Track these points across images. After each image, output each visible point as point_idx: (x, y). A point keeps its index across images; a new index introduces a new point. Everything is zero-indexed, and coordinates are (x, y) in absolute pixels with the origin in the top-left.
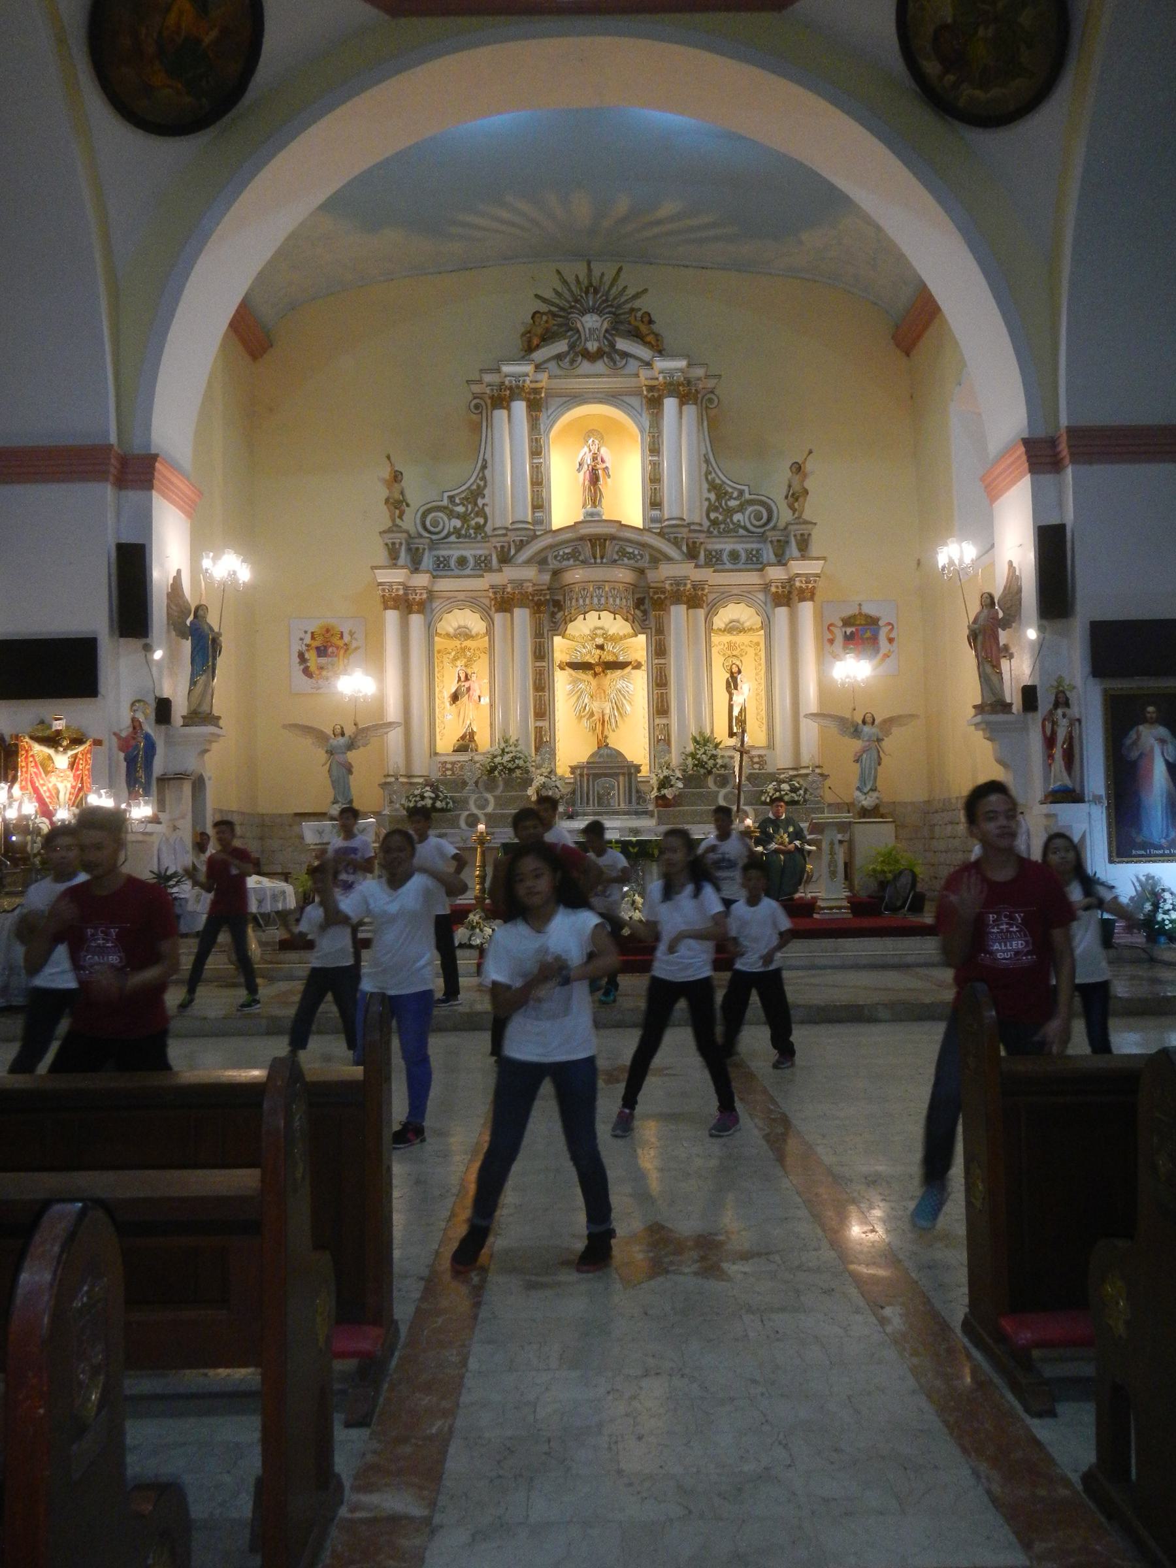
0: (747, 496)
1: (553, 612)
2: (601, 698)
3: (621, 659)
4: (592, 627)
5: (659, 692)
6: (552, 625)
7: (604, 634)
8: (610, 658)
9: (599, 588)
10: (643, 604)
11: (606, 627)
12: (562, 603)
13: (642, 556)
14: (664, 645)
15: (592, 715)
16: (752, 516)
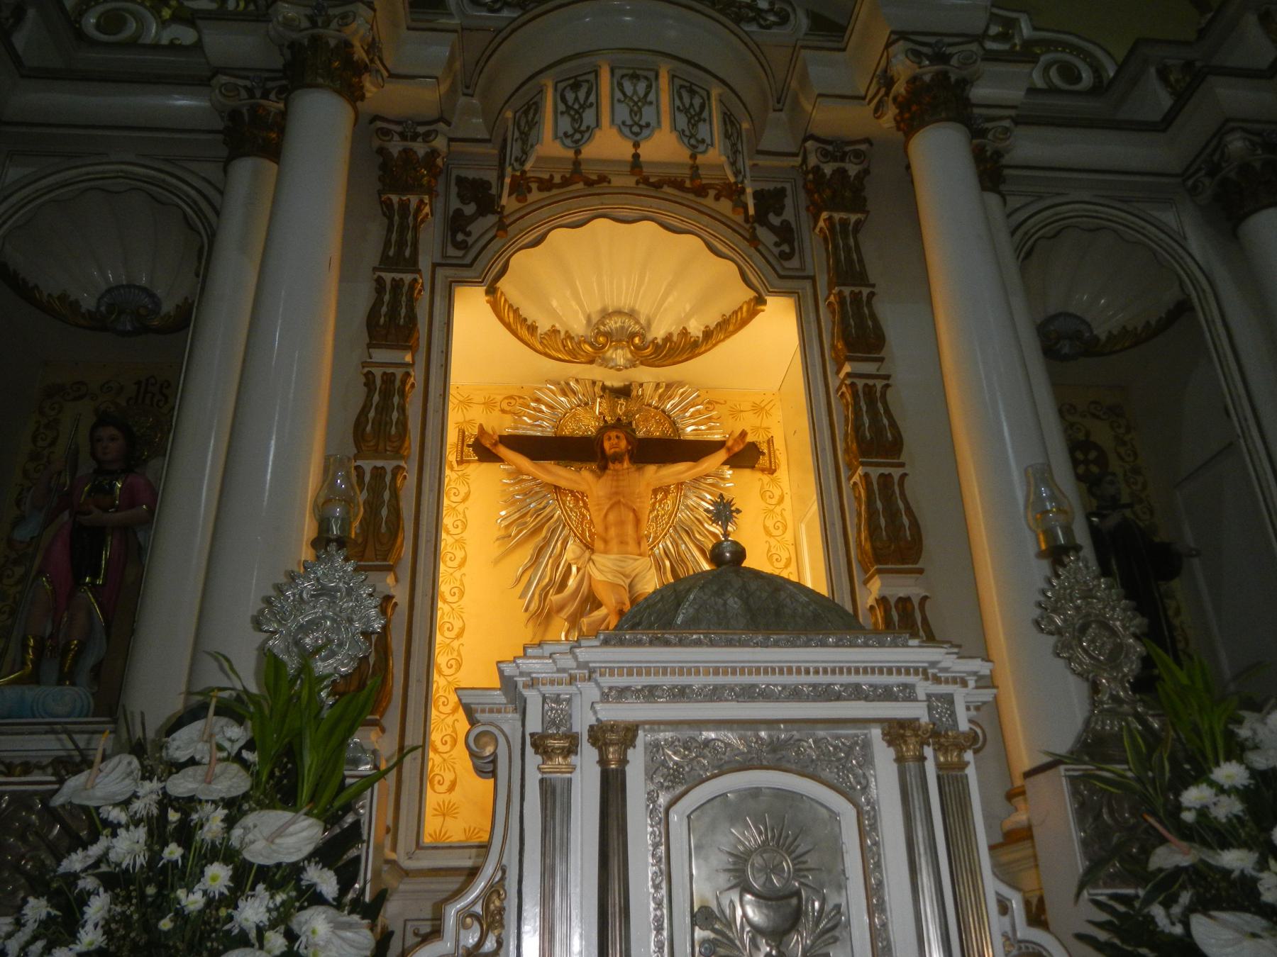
0: (1026, 30)
1: (458, 212)
2: (623, 542)
3: (689, 431)
4: (594, 308)
5: (875, 473)
6: (452, 251)
7: (632, 336)
8: (648, 428)
9: (635, 77)
10: (779, 213)
11: (644, 310)
12: (494, 191)
13: (784, 19)
14: (873, 316)
15: (592, 601)
16: (1053, 72)
